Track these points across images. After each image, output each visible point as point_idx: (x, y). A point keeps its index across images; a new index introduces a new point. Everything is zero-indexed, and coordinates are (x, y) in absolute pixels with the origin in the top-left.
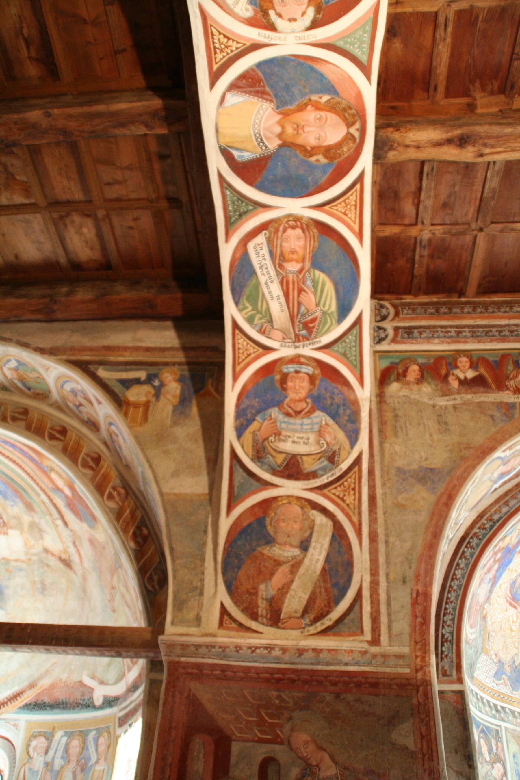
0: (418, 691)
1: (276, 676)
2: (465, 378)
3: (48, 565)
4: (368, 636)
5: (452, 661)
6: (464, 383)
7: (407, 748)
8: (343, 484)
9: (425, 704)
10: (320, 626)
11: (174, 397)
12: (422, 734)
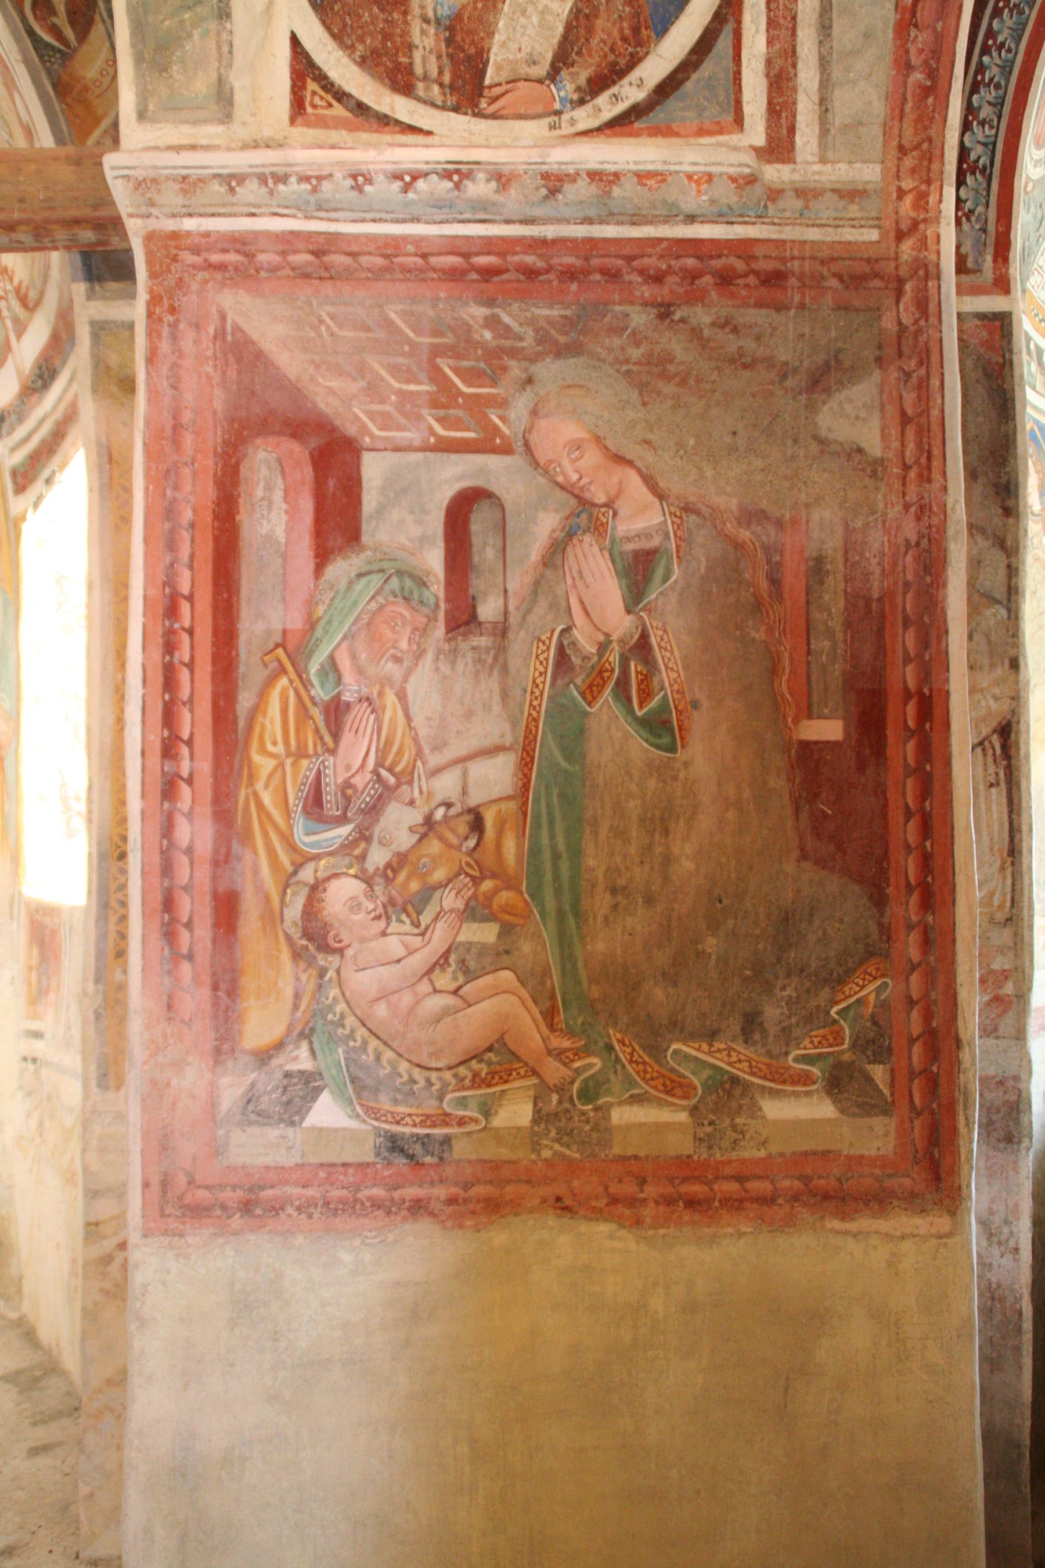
0: (899, 294)
1: (482, 260)
4: (756, 132)
5: (984, 230)
7: (860, 450)
9: (918, 332)
12: (903, 413)
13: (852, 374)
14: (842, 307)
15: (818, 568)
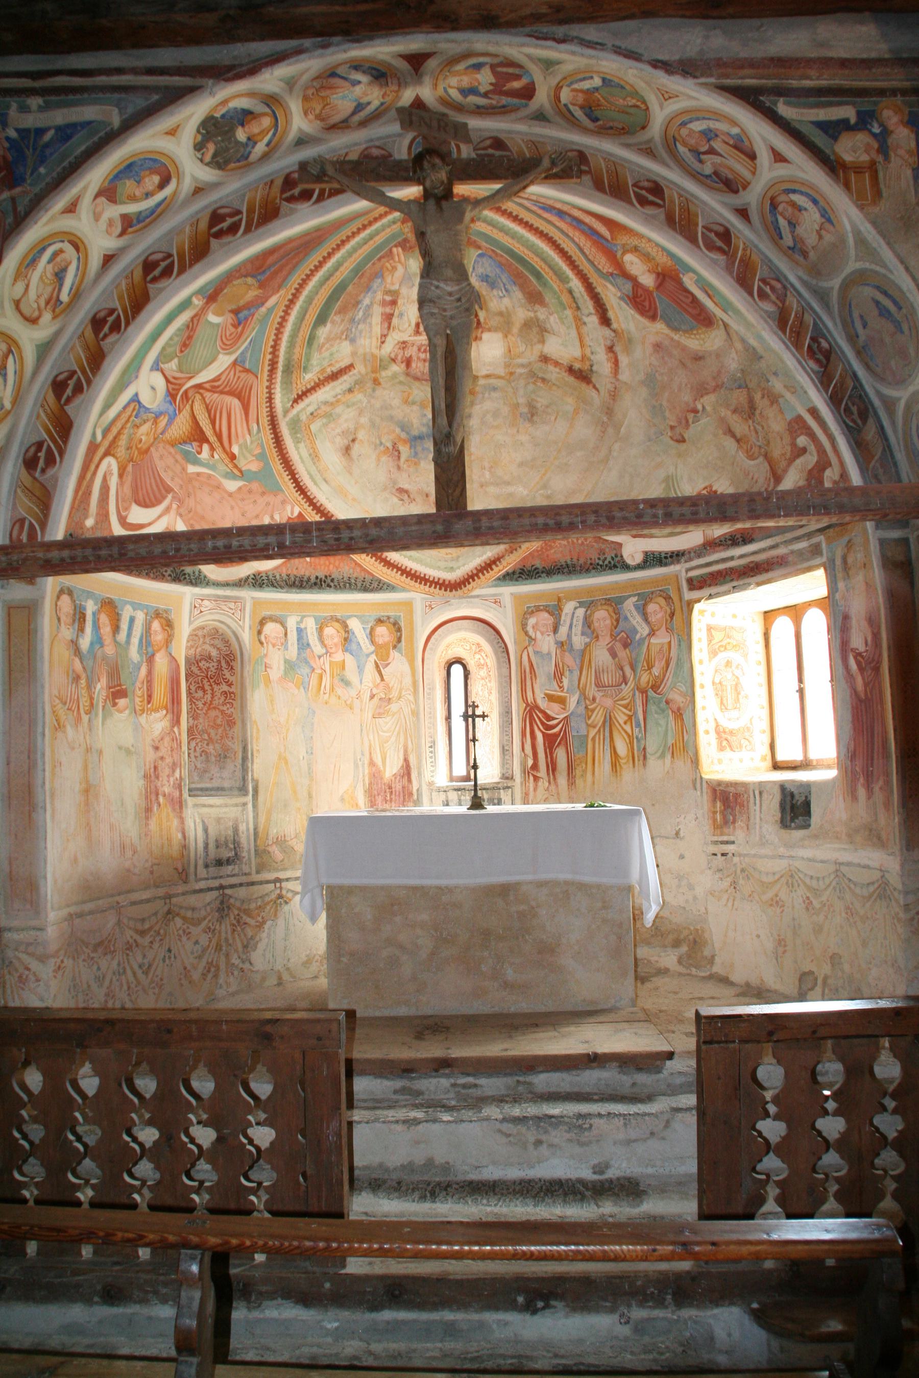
3: (543, 380)
11: (910, 152)
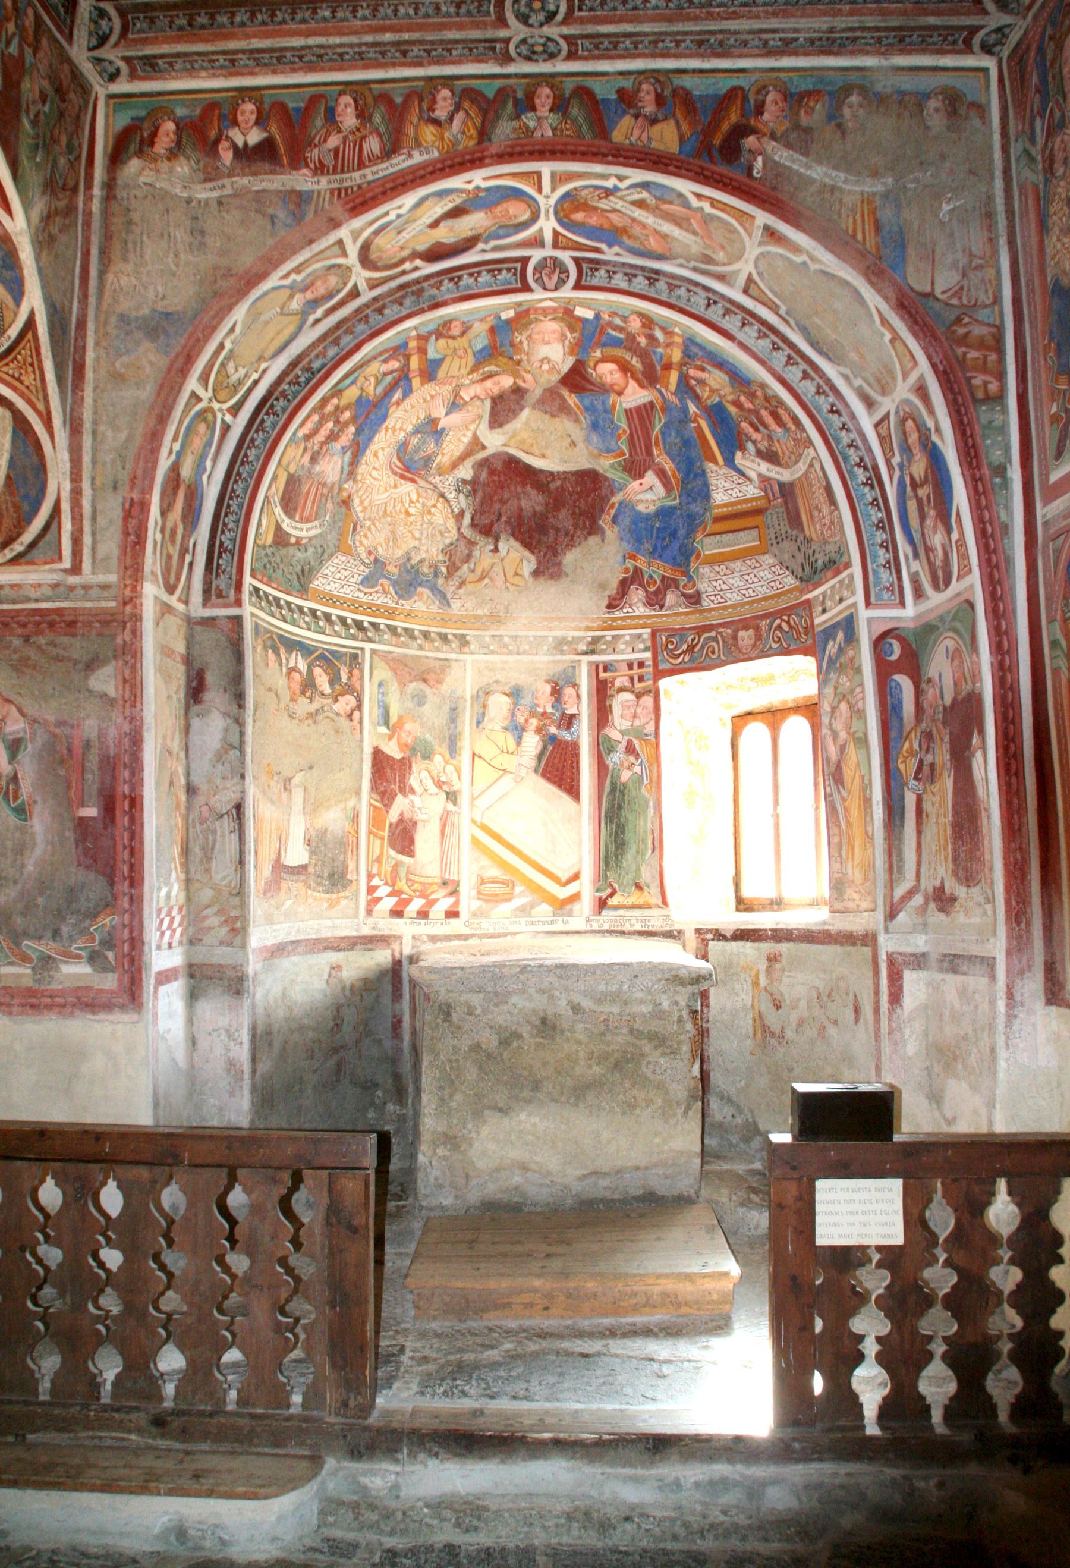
0: (124, 628)
2: (246, 144)
4: (67, 564)
6: (245, 155)
8: (15, 358)
10: (9, 554)
13: (104, 662)
14: (100, 635)
15: (87, 744)
